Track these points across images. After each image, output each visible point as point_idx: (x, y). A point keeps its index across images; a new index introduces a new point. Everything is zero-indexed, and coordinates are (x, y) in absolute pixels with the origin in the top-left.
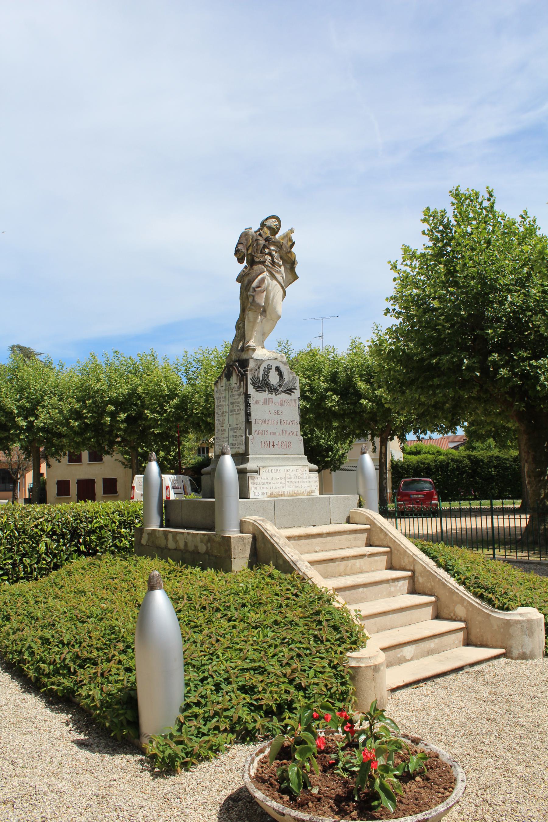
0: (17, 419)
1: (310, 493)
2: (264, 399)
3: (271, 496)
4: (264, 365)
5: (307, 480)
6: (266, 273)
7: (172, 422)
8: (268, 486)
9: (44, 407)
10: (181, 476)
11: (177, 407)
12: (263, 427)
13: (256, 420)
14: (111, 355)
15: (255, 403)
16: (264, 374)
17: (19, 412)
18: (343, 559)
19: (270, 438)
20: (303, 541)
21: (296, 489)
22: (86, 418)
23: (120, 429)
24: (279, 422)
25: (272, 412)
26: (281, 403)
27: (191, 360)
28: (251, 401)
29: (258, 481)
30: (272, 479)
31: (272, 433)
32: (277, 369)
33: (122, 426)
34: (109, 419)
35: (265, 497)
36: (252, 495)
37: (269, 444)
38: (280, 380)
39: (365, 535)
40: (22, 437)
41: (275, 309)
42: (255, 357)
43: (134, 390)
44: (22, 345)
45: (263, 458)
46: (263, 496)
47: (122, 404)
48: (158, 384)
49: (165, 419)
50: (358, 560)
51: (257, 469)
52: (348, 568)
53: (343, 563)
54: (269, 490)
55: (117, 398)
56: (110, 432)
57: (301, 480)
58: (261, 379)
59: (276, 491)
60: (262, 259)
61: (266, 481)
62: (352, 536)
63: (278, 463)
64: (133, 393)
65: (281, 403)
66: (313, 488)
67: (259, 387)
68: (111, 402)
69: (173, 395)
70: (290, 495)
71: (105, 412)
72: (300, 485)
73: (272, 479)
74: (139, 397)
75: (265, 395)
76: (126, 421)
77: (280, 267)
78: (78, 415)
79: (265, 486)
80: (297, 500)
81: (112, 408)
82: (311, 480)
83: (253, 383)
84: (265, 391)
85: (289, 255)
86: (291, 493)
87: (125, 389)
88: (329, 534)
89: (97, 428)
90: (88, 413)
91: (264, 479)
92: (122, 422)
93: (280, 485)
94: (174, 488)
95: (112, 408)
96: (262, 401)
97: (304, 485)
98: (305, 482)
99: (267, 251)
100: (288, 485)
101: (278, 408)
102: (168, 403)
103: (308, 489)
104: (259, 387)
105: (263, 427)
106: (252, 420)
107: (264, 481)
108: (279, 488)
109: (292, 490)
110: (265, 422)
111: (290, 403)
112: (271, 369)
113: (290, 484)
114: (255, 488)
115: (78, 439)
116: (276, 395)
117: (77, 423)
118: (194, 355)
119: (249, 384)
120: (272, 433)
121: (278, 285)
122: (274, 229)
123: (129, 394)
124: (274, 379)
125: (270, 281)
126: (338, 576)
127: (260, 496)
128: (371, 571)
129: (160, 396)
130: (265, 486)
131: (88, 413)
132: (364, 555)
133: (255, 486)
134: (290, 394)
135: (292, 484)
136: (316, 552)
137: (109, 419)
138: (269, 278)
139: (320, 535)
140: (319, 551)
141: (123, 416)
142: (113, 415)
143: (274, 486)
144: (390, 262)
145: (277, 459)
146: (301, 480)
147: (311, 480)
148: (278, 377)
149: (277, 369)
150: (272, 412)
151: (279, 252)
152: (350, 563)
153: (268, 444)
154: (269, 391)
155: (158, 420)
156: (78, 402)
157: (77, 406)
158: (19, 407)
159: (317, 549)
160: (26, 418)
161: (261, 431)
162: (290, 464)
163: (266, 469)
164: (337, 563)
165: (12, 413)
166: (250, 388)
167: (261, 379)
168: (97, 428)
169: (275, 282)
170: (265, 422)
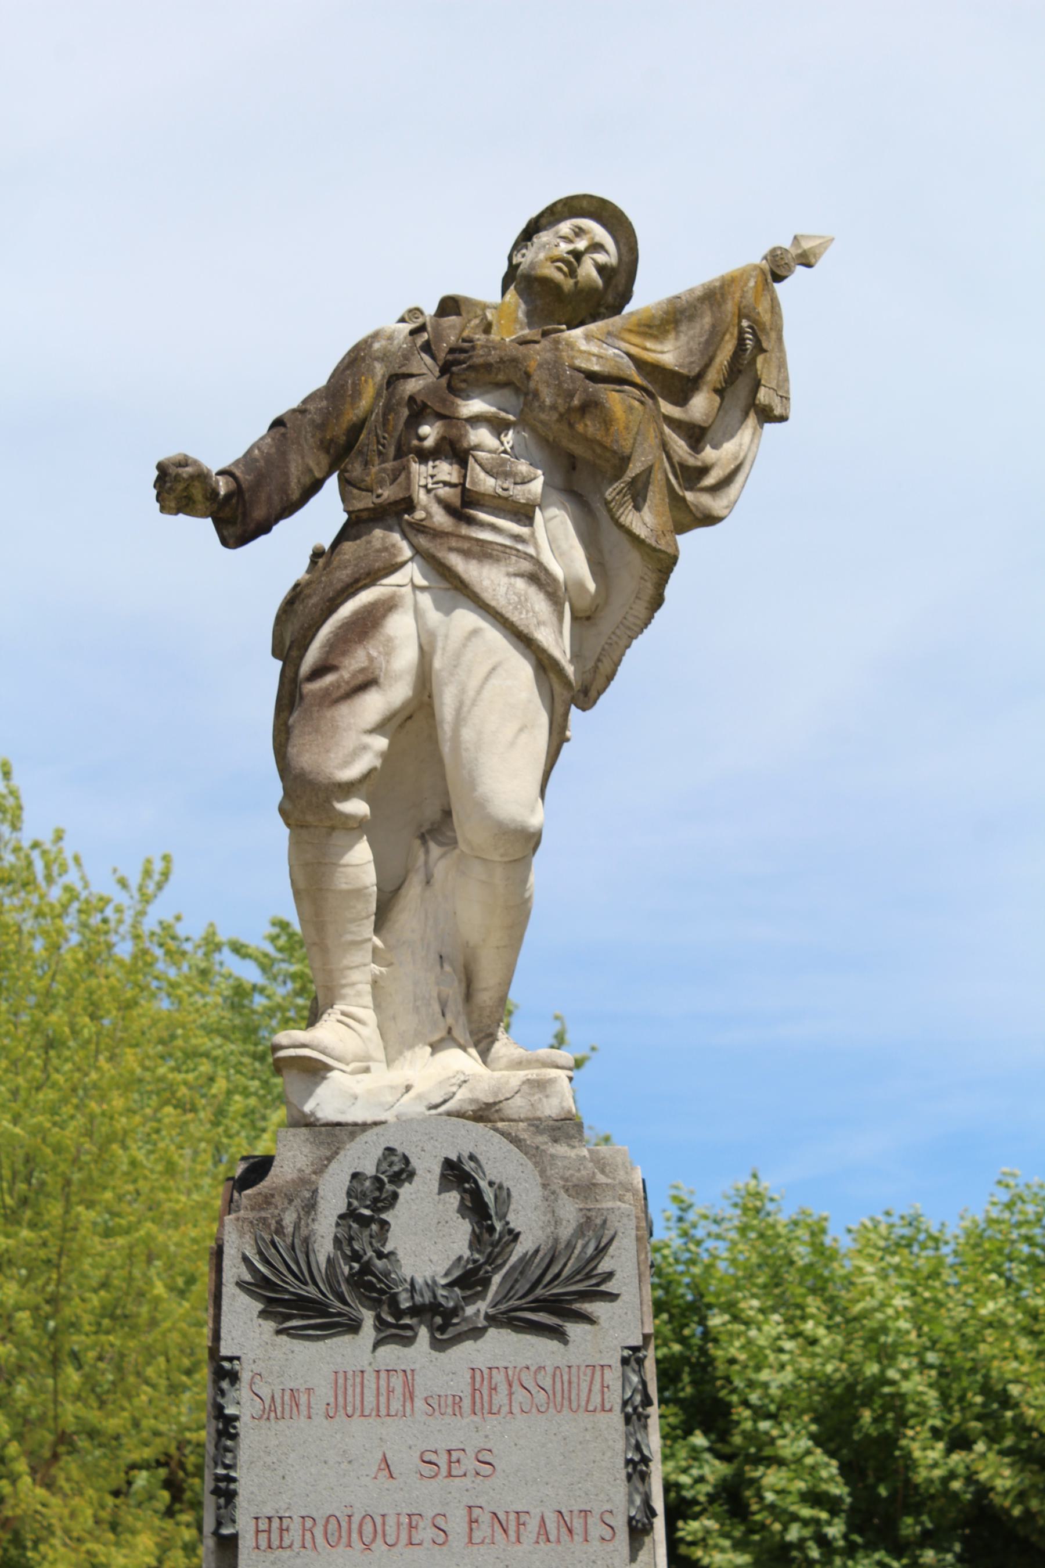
2: (340, 1380)
4: (362, 1157)
6: (412, 572)
13: (274, 1529)
15: (270, 1412)
16: (350, 1215)
24: (457, 1525)
25: (406, 1461)
28: (242, 1404)
32: (456, 1174)
38: (476, 1242)
41: (472, 784)
58: (324, 1249)
60: (388, 493)
65: (481, 1394)
67: (304, 1306)
75: (356, 1351)
77: (524, 514)
83: (260, 1287)
84: (354, 1327)
85: (589, 427)
96: (324, 1392)
99: (430, 432)
101: (459, 1432)
104: (304, 1306)
106: (244, 1525)
111: (561, 1394)
112: (404, 1173)
116: (439, 1345)
119: (229, 1289)
121: (494, 636)
122: (546, 282)
124: (426, 1241)
125: (434, 617)
134: (558, 1334)
138: (425, 600)
148: (463, 1229)
149: (456, 1174)
150: (406, 1461)
151: (522, 422)
154: (381, 1324)
166: (241, 1313)
167: (324, 1249)
169: (466, 618)
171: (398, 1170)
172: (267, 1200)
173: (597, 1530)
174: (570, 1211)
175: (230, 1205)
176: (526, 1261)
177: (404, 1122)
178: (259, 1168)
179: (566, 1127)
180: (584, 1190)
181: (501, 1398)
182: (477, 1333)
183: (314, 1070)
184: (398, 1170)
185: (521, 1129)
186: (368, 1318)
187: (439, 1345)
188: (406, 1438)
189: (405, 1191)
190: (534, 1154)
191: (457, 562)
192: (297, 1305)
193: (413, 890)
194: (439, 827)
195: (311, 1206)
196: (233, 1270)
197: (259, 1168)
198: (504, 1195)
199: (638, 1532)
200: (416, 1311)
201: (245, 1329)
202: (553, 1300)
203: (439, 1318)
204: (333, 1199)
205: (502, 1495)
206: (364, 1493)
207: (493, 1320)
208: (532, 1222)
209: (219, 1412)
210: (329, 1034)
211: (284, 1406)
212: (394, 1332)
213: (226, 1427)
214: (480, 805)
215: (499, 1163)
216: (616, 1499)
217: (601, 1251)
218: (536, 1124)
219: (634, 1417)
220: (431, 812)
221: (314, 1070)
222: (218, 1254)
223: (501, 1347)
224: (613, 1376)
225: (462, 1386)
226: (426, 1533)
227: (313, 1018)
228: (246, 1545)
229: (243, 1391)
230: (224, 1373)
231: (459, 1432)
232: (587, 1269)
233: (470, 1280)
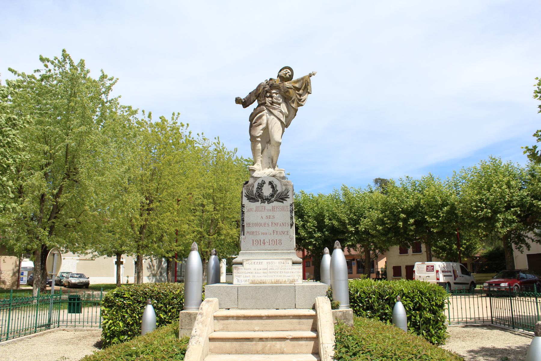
0: (348, 227)
1: (293, 281)
2: (257, 207)
3: (253, 283)
4: (259, 181)
5: (290, 271)
6: (266, 111)
7: (446, 223)
8: (251, 275)
9: (365, 218)
10: (451, 264)
11: (448, 212)
12: (254, 229)
13: (249, 224)
14: (404, 179)
15: (248, 211)
16: (258, 188)
17: (349, 222)
18: (261, 339)
19: (262, 238)
20: (241, 321)
21: (278, 278)
22: (387, 223)
23: (411, 230)
24: (270, 224)
25: (264, 217)
26: (273, 209)
27: (458, 177)
28: (245, 210)
29: (241, 271)
30: (255, 269)
31: (263, 234)
32: (270, 183)
33: (412, 228)
34: (401, 223)
35: (247, 284)
36: (235, 282)
37: (259, 242)
38: (273, 191)
39: (311, 321)
40: (352, 238)
41: (273, 137)
42: (255, 176)
43: (419, 203)
44: (382, 178)
45: (252, 253)
46: (245, 283)
47: (410, 213)
48: (434, 198)
49: (441, 222)
50: (278, 342)
51: (241, 261)
52: (267, 348)
53: (261, 343)
54: (251, 278)
55: (407, 208)
56: (405, 232)
57: (283, 271)
58: (255, 192)
59: (258, 279)
60: (263, 102)
61: (249, 271)
62: (295, 321)
63: (260, 257)
64: (418, 205)
65: (273, 209)
66: (296, 278)
67: (252, 198)
68: (403, 212)
69: (444, 204)
70: (272, 283)
71: (400, 219)
72: (282, 274)
73: (255, 269)
74: (422, 207)
75: (258, 204)
76: (415, 223)
77: (279, 104)
78: (381, 222)
79: (247, 275)
80: (261, 287)
81: (403, 216)
82: (293, 270)
83: (247, 196)
84: (258, 201)
85: (287, 94)
86: (273, 281)
87: (412, 202)
88: (269, 317)
89: (395, 229)
90: (387, 220)
91: (247, 269)
92: (412, 225)
93: (262, 275)
94: (443, 272)
95: (403, 216)
96: (255, 209)
97: (286, 275)
98: (287, 273)
99: (268, 94)
100: (270, 274)
101: (271, 213)
102: (441, 210)
103: (291, 278)
105: (254, 229)
106: (245, 224)
107: (247, 271)
108: (260, 277)
109: (274, 279)
110: (256, 225)
111: (283, 209)
112: (264, 183)
113: (272, 274)
114: (239, 276)
115: (384, 239)
116: (268, 203)
117: (381, 228)
118: (460, 173)
120: (263, 234)
121: (276, 119)
122: (282, 77)
123: (416, 206)
124: (267, 191)
125: (268, 116)
126: (255, 354)
127: (243, 283)
128: (294, 353)
129: (436, 205)
130: (247, 275)
131: (387, 220)
132: (288, 339)
133: (239, 275)
134: (282, 202)
135: (274, 274)
136: (255, 331)
137: (401, 223)
139: (260, 317)
140: (258, 331)
141: (412, 221)
142: (405, 221)
143: (256, 275)
144: (537, 78)
145: (266, 253)
146: (283, 271)
147: (293, 270)
148: (272, 189)
149: (270, 183)
150: (264, 217)
152: (269, 344)
153: (259, 242)
154: (261, 201)
155: (435, 223)
156: (382, 213)
157: (381, 216)
158: (349, 219)
159: (257, 328)
160: (354, 225)
161: (253, 233)
162: (275, 257)
163: (250, 262)
164: (254, 342)
165: (345, 223)
167: (255, 192)
168: (395, 229)
169: (272, 117)
170: (256, 225)
171: (263, 183)
172: (248, 186)
173: (287, 225)
174: (284, 188)
175: (244, 187)
176: (279, 194)
177: (264, 177)
178: (247, 182)
179: (284, 178)
180: (286, 185)
181: (276, 209)
182: (273, 202)
183: (254, 171)
184: (263, 183)
185: (278, 178)
186: (260, 200)
187: (268, 203)
188: (264, 214)
189: (264, 185)
190: (280, 181)
191: (271, 110)
192: (251, 199)
193: (266, 149)
194: (269, 142)
195: (253, 187)
196: (244, 194)
197: (247, 182)
198: (276, 186)
199: (292, 225)
200: (265, 199)
201: (245, 201)
202: (282, 198)
203: (268, 200)
204: (256, 186)
205: (276, 221)
206: (259, 220)
207: (275, 200)
208: (279, 189)
209: (242, 211)
210: (255, 167)
211: (250, 210)
212: (263, 202)
213: (243, 213)
214: (274, 139)
215: (276, 182)
216: (289, 221)
217: (288, 192)
218: (280, 177)
219: (291, 212)
220: (268, 140)
221: (254, 171)
222: (242, 192)
223: (276, 204)
224: (289, 207)
225: (271, 208)
226: (267, 225)
227: (254, 165)
228: (245, 226)
229: (245, 208)
230: (243, 206)
231: (271, 213)
232: (286, 195)
233: (272, 196)
